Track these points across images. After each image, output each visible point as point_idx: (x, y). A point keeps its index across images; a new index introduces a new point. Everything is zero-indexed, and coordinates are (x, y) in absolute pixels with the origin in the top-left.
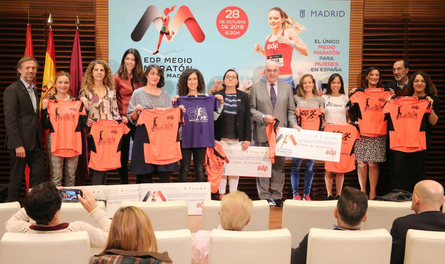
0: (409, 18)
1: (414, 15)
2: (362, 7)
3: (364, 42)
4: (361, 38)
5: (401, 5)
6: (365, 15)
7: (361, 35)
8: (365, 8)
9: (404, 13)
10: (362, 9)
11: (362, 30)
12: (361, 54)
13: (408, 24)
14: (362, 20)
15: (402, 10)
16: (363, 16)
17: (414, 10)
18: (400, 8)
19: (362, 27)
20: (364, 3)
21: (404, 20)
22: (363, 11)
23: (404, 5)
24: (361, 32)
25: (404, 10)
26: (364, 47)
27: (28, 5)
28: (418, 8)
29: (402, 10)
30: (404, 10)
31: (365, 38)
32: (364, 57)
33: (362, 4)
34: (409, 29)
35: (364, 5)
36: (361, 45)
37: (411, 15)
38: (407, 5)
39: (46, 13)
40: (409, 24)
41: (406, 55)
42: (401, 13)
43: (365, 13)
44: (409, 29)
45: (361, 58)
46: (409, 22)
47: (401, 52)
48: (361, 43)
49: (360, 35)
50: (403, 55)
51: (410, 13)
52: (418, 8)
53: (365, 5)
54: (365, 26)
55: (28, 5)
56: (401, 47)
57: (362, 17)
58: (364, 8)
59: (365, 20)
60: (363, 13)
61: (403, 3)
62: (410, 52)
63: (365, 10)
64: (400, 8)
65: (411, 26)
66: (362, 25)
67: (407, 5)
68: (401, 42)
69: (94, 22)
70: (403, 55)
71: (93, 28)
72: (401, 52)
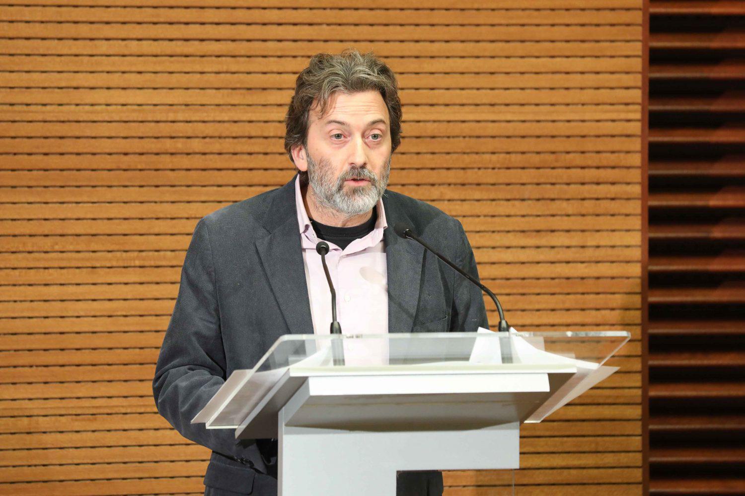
45: (638, 32)
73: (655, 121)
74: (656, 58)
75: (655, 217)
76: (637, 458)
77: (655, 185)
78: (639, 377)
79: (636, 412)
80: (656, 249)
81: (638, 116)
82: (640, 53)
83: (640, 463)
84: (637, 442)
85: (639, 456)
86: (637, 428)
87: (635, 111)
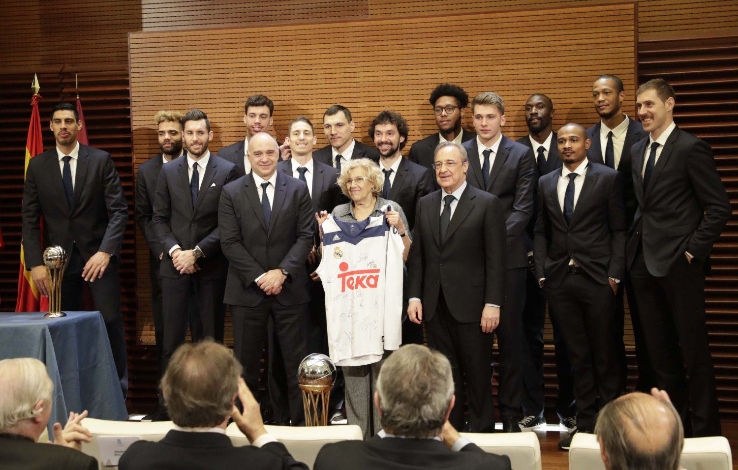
2: (632, 17)
10: (633, 22)
11: (633, 66)
14: (633, 44)
16: (636, 37)
19: (633, 60)
27: (39, 58)
33: (632, 12)
39: (63, 69)
43: (640, 30)
53: (640, 14)
54: (640, 57)
55: (39, 58)
57: (632, 39)
59: (639, 45)
63: (640, 25)
66: (632, 55)
69: (127, 83)
71: (127, 93)
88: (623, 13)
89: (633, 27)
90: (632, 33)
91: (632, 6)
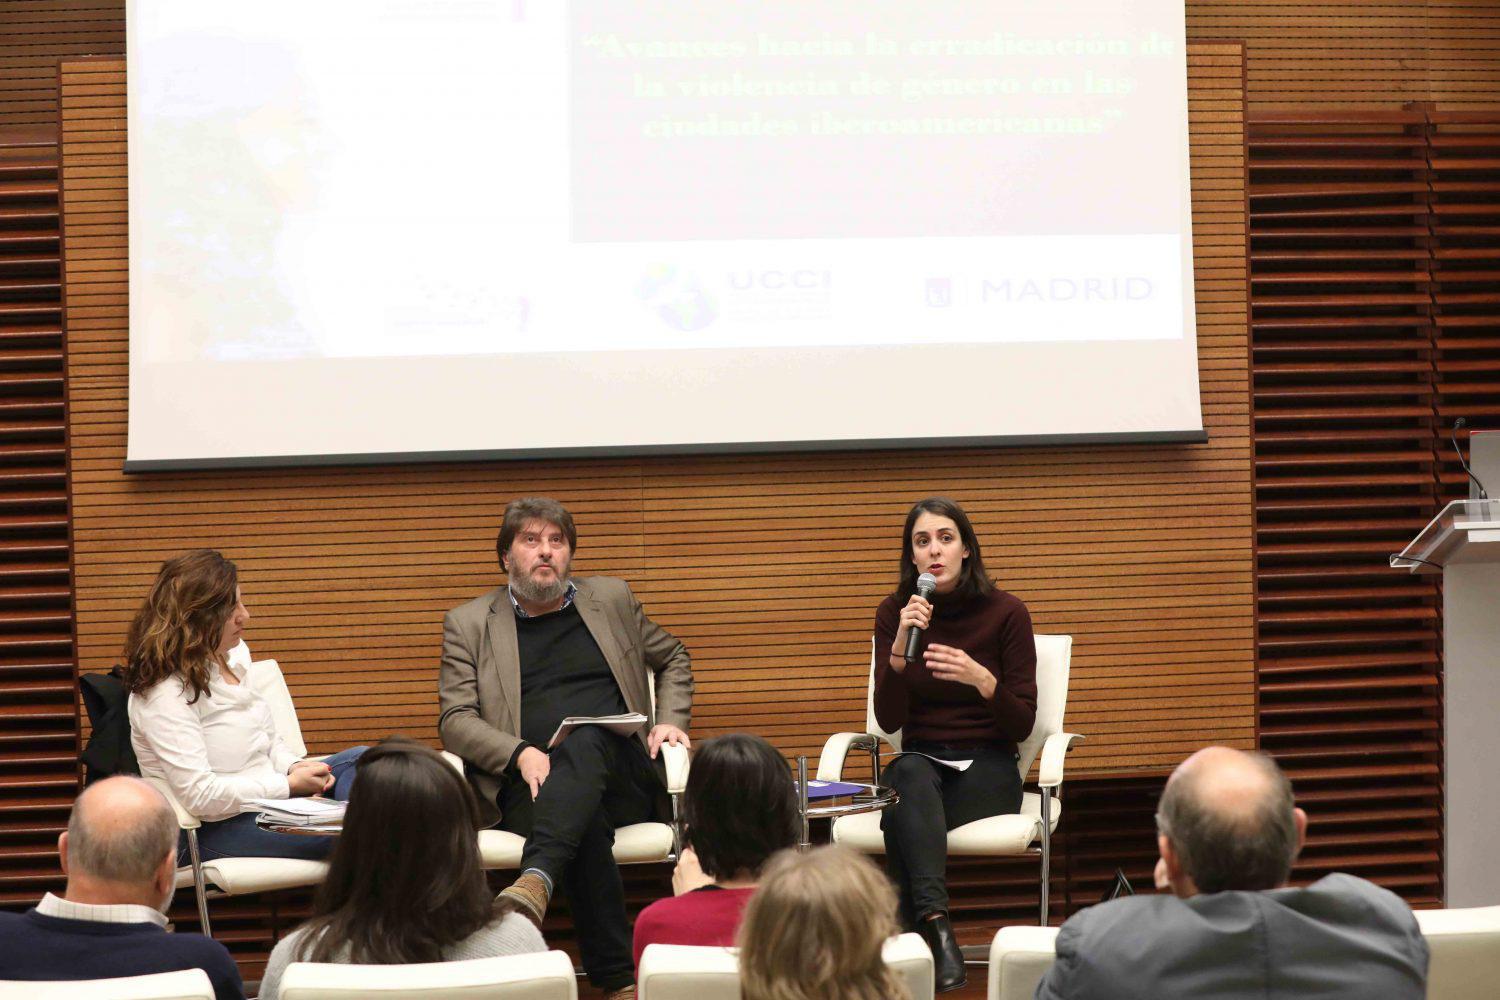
0: (1432, 121)
1: (1452, 108)
2: (1238, 72)
3: (1255, 224)
4: (1241, 207)
5: (1395, 64)
6: (1252, 107)
7: (1241, 195)
8: (1250, 75)
9: (1409, 97)
11: (1241, 173)
12: (1244, 276)
13: (1429, 147)
14: (1240, 128)
15: (1403, 86)
16: (1244, 111)
17: (1449, 85)
18: (1392, 76)
19: (1240, 162)
20: (1243, 55)
21: (1411, 131)
22: (1243, 89)
23: (1408, 64)
24: (1240, 183)
25: (1411, 86)
26: (1255, 245)
28: (1465, 75)
29: (1403, 86)
30: (1411, 86)
31: (1255, 205)
32: (1257, 290)
33: (1238, 61)
34: (1437, 165)
35: (1244, 67)
36: (1242, 240)
37: (1440, 108)
38: (1418, 64)
40: (1435, 143)
41: (1429, 279)
42: (1398, 96)
44: (1437, 165)
45: (1243, 296)
46: (1438, 135)
47: (1409, 266)
48: (1242, 229)
49: (1235, 191)
50: (1418, 277)
51: (1434, 97)
52: (1465, 75)
54: (1253, 153)
56: (1408, 243)
57: (1238, 116)
58: (1244, 78)
59: (1253, 130)
60: (1245, 100)
61: (1403, 54)
62: (1447, 265)
64: (1392, 76)
65: (1443, 153)
66: (1240, 150)
67: (1418, 64)
68: (1408, 221)
69: (54, 176)
70: (1418, 277)
71: (53, 201)
72: (1409, 266)
73: (1257, 359)
74: (1257, 314)
75: (1259, 427)
76: (1250, 599)
77: (1259, 404)
78: (1250, 541)
79: (1249, 565)
80: (1261, 450)
81: (1246, 355)
82: (1245, 310)
83: (1251, 602)
84: (1249, 587)
85: (1251, 597)
86: (1249, 577)
87: (1244, 351)
88: (1220, 61)
89: (1240, 93)
90: (1239, 105)
91: (1237, 49)
